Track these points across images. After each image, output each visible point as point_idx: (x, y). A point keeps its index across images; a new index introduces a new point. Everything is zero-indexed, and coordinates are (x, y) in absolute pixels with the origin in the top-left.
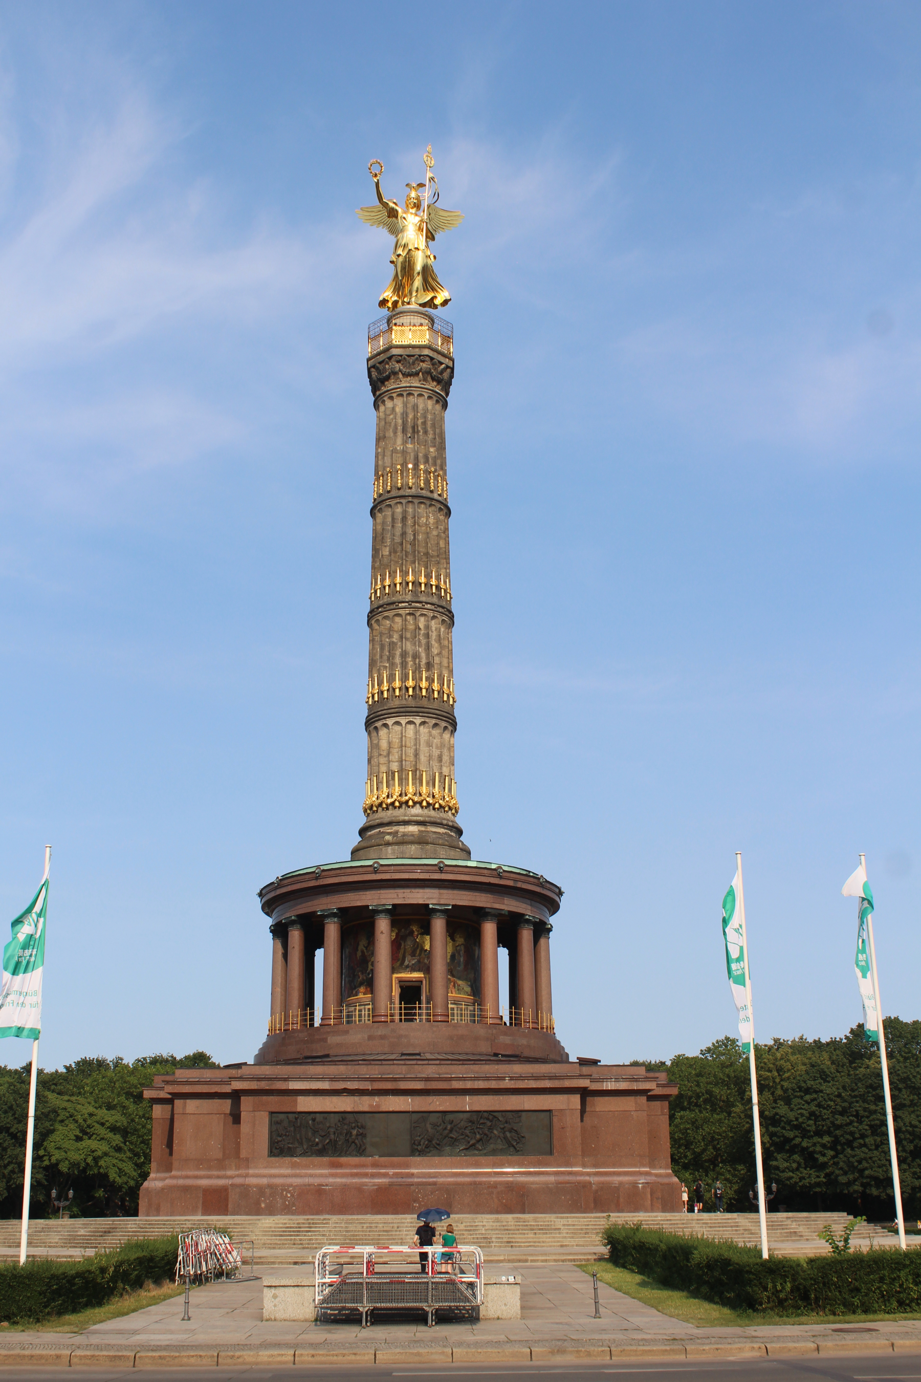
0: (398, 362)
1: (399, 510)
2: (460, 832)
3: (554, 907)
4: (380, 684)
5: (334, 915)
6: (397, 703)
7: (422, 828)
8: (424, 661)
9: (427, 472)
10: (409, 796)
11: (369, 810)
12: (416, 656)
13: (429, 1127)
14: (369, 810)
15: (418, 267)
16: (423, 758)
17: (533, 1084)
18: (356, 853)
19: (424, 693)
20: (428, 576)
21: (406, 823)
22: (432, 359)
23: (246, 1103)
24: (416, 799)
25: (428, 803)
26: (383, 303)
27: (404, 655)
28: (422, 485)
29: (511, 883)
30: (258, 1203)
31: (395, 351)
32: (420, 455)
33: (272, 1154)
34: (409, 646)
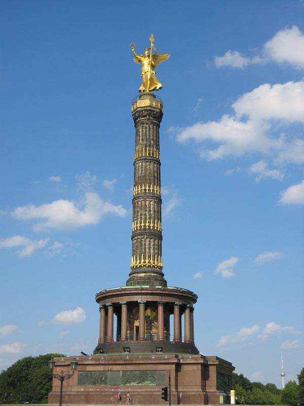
1: (140, 164)
2: (163, 275)
5: (110, 306)
6: (138, 232)
7: (146, 274)
8: (148, 217)
9: (150, 150)
11: (133, 268)
12: (145, 215)
13: (127, 376)
19: (147, 227)
20: (150, 187)
24: (144, 264)
27: (141, 215)
28: (147, 155)
31: (138, 109)
32: (147, 144)
33: (78, 384)
34: (143, 213)
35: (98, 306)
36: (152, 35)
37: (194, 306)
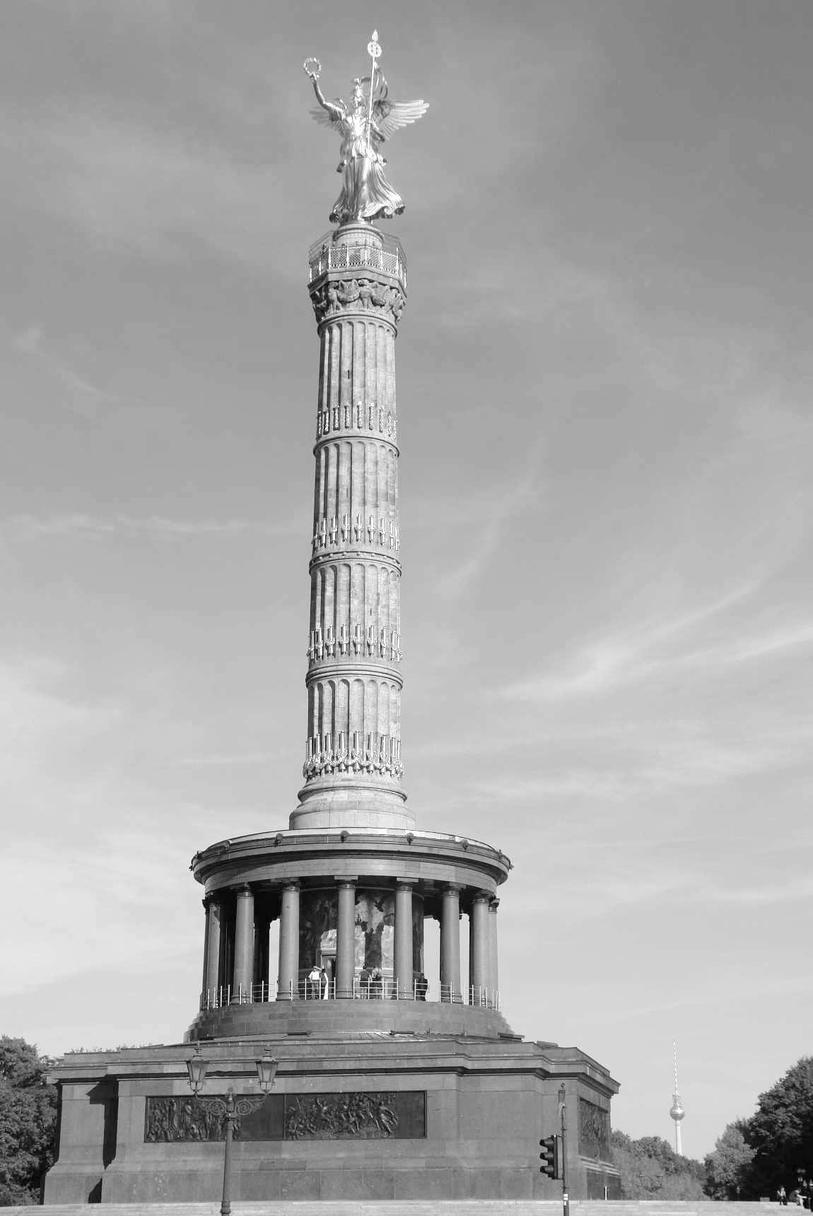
0: (336, 288)
3: (499, 875)
4: (317, 641)
10: (341, 760)
14: (311, 773)
15: (365, 176)
16: (355, 718)
17: (405, 1065)
18: (293, 817)
21: (333, 789)
22: (371, 281)
23: (124, 1088)
25: (362, 767)
26: (333, 218)
29: (424, 850)
30: (130, 1190)
33: (147, 1139)
35: (201, 890)
36: (375, 36)
37: (500, 891)
